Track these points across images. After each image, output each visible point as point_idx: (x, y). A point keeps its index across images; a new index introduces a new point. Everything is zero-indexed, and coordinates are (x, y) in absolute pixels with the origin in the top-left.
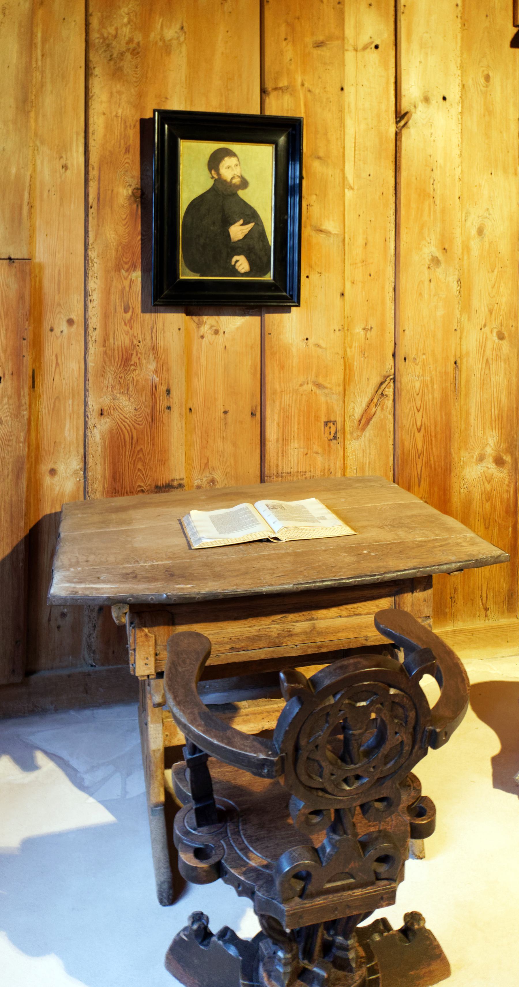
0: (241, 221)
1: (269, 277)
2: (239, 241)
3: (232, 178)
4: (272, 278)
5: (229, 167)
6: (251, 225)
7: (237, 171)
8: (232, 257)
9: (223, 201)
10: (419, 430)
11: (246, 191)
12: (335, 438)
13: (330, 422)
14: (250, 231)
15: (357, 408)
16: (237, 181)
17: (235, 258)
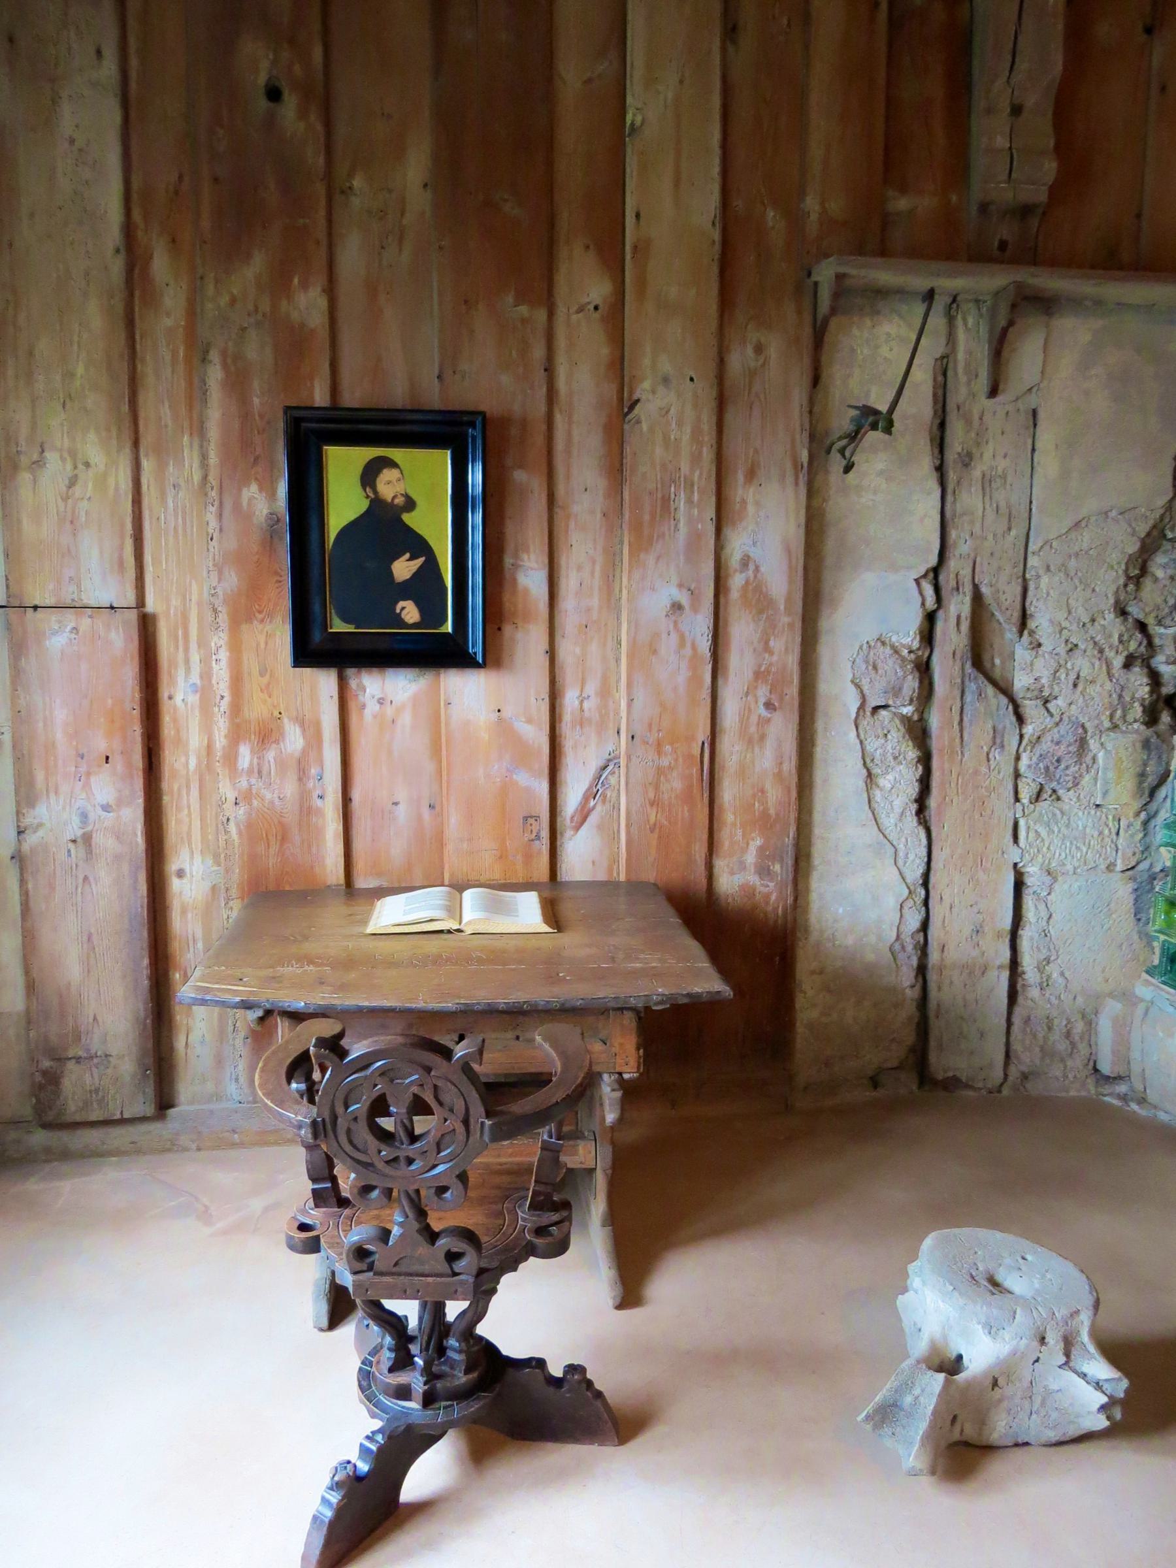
0: (407, 555)
2: (407, 581)
3: (394, 497)
4: (450, 630)
5: (389, 483)
6: (421, 560)
7: (400, 488)
8: (396, 603)
9: (385, 528)
10: (652, 830)
11: (413, 514)
12: (538, 837)
13: (531, 817)
14: (421, 567)
16: (400, 501)
17: (401, 604)
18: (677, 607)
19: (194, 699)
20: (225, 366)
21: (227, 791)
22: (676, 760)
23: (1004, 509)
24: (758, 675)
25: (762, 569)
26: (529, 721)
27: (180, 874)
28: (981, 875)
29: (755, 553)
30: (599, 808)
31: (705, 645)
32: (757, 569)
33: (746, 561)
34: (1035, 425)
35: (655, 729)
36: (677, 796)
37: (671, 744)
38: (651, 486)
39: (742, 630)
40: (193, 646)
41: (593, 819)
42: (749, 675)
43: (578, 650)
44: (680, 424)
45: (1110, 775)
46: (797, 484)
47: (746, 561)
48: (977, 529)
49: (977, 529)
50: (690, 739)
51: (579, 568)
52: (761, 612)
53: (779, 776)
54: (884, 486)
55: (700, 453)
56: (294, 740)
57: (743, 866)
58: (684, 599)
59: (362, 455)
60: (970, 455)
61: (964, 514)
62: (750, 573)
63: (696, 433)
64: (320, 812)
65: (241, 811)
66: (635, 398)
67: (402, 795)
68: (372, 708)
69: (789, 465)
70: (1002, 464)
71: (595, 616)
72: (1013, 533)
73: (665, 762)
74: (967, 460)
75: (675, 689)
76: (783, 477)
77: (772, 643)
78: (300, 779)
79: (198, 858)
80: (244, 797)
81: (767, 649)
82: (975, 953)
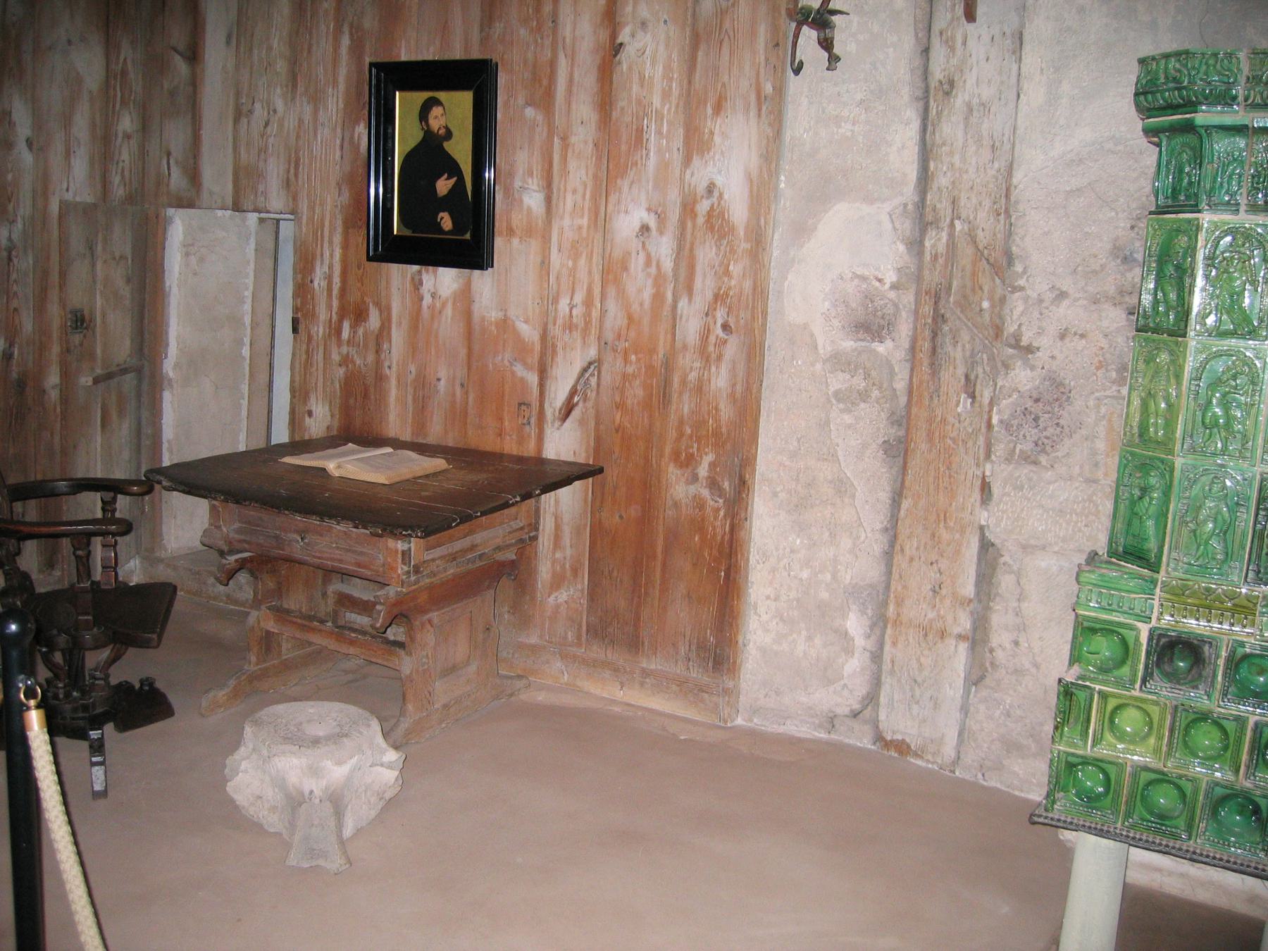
1: (468, 236)
7: (442, 122)
9: (430, 156)
10: (617, 431)
15: (559, 393)
17: (441, 214)
18: (645, 229)
19: (324, 284)
20: (351, 34)
21: (336, 357)
22: (639, 369)
23: (986, 142)
24: (716, 297)
25: (726, 197)
26: (526, 322)
27: (310, 414)
28: (945, 535)
29: (719, 181)
30: (581, 405)
31: (668, 265)
32: (721, 195)
33: (711, 189)
34: (1021, 44)
35: (623, 339)
36: (639, 403)
37: (636, 354)
38: (628, 119)
39: (707, 254)
40: (326, 245)
41: (576, 413)
42: (709, 295)
43: (570, 263)
44: (653, 64)
45: (1101, 445)
46: (759, 116)
47: (711, 189)
48: (956, 160)
49: (956, 160)
50: (653, 351)
51: (574, 192)
52: (721, 237)
53: (732, 395)
54: (863, 117)
55: (671, 88)
56: (374, 321)
57: (695, 478)
58: (652, 221)
59: (421, 96)
60: (952, 83)
61: (944, 144)
62: (715, 200)
63: (668, 68)
64: (387, 377)
65: (341, 371)
66: (619, 41)
67: (443, 374)
68: (427, 300)
69: (753, 98)
70: (987, 92)
71: (584, 235)
72: (996, 165)
73: (630, 370)
74: (949, 87)
75: (641, 305)
76: (747, 109)
77: (731, 268)
78: (377, 352)
79: (320, 406)
80: (346, 360)
81: (727, 273)
82: (931, 615)
